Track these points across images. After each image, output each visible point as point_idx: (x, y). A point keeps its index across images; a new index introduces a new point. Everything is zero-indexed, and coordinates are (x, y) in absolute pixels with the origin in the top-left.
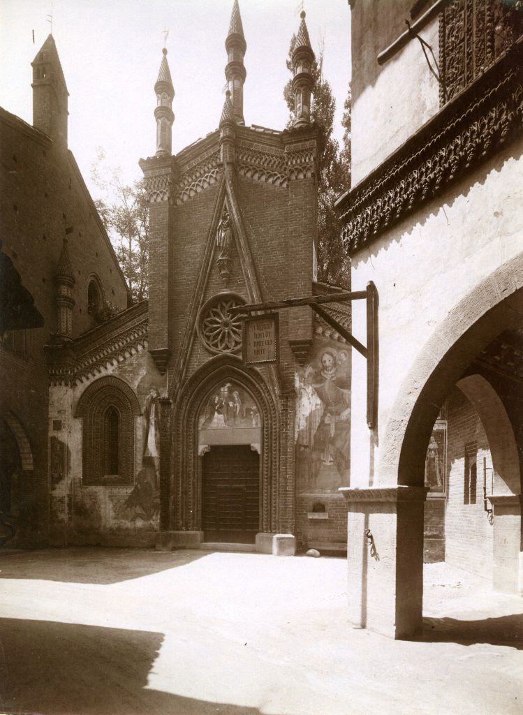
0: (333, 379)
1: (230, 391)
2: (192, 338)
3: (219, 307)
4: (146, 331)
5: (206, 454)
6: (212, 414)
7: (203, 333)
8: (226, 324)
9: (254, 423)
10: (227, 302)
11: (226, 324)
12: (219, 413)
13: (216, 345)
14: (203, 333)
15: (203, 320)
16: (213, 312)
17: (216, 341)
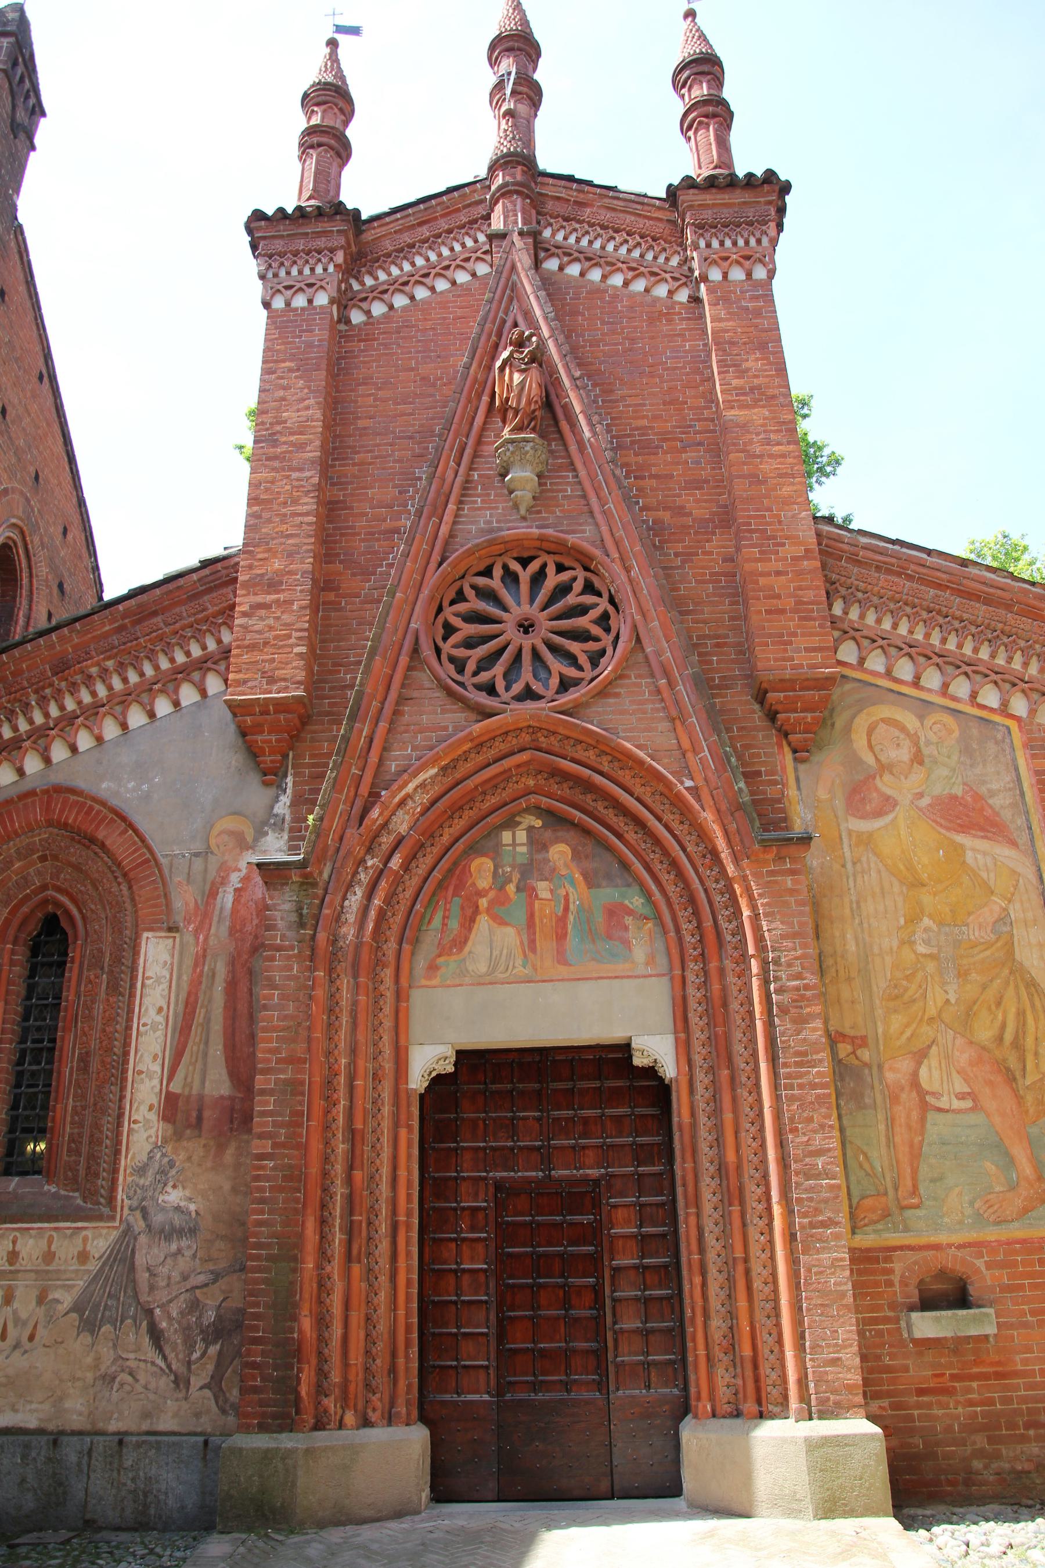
0: (925, 802)
1: (538, 845)
2: (404, 660)
3: (498, 572)
4: (219, 642)
5: (438, 1081)
6: (469, 921)
7: (438, 651)
8: (526, 627)
9: (640, 953)
10: (525, 562)
11: (526, 627)
12: (503, 923)
13: (491, 690)
14: (438, 651)
15: (440, 609)
16: (473, 587)
17: (484, 677)
